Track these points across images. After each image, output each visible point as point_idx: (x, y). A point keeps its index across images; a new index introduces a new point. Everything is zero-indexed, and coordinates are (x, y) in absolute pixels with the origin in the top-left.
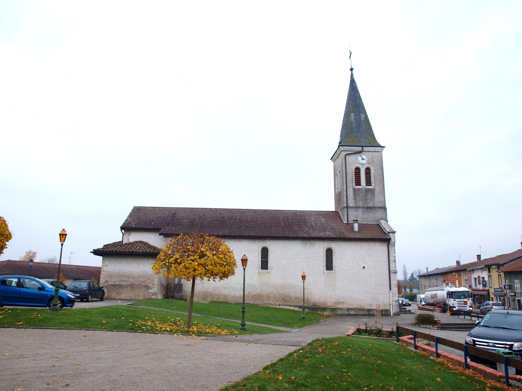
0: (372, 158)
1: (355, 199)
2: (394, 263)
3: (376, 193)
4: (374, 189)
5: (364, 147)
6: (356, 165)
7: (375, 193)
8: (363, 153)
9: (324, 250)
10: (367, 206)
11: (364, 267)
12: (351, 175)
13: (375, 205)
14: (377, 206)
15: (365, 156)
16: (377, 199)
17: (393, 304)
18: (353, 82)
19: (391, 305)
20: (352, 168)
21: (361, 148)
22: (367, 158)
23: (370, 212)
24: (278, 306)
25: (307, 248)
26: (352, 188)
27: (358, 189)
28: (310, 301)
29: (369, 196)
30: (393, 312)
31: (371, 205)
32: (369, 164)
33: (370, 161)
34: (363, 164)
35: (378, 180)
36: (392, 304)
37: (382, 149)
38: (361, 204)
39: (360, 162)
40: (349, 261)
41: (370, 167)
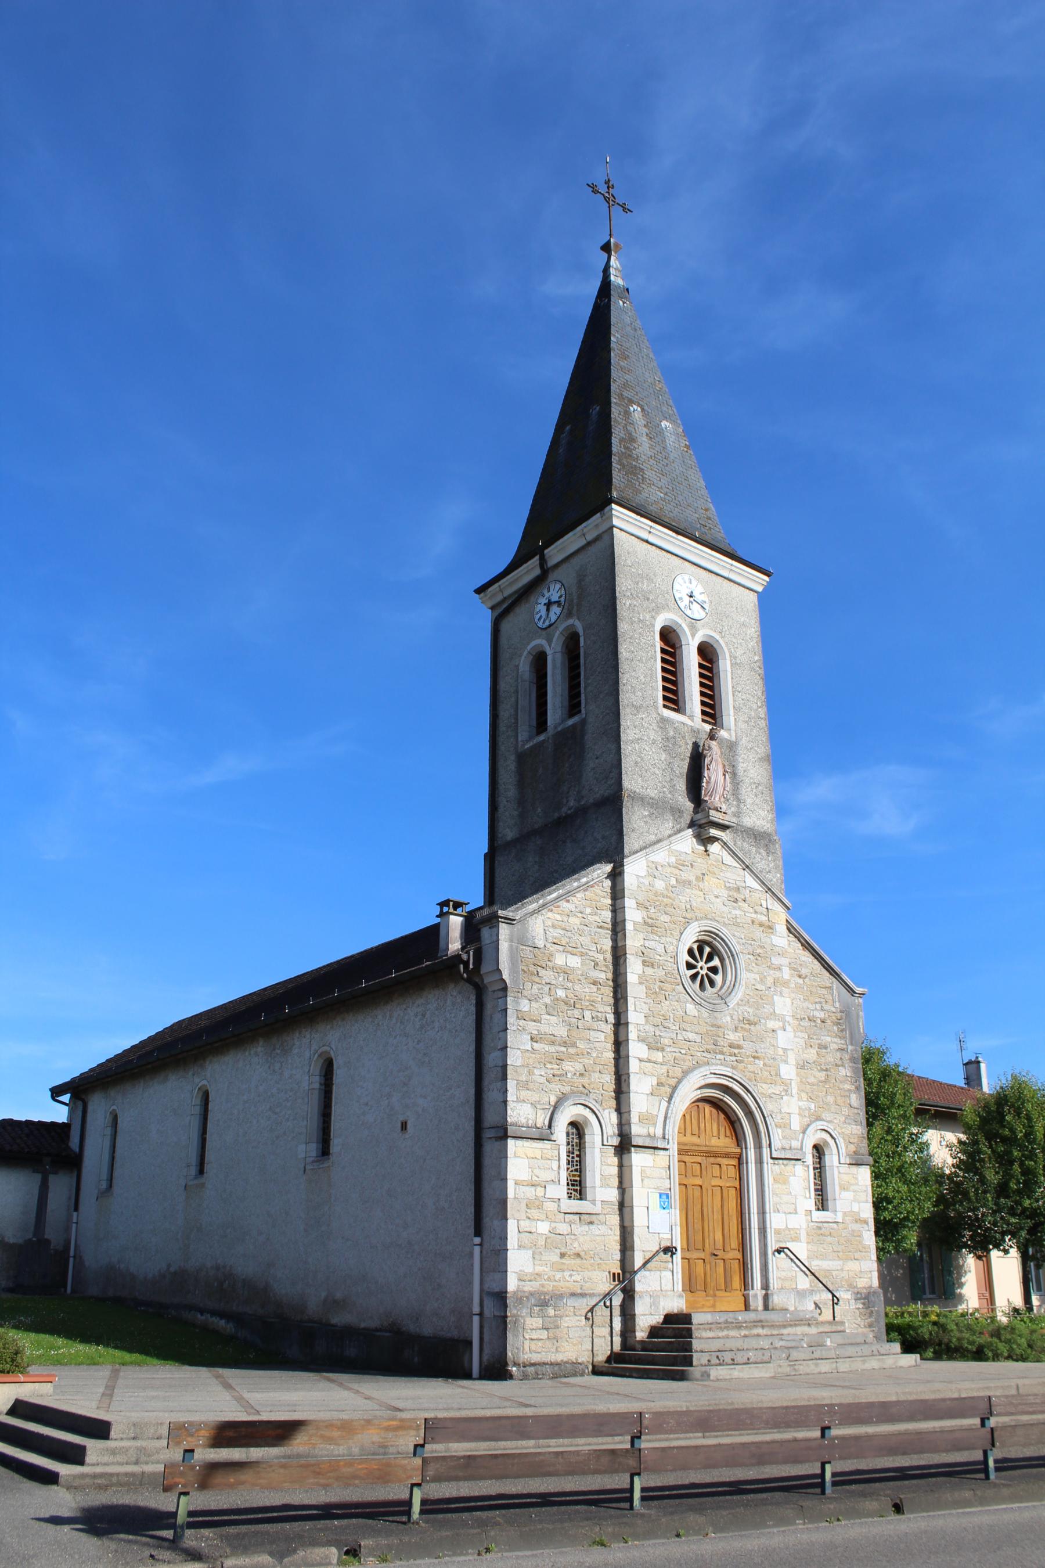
0: (581, 579)
1: (521, 802)
2: (499, 1084)
3: (589, 737)
4: (583, 722)
5: (546, 551)
6: (528, 644)
7: (586, 737)
8: (552, 576)
9: (310, 1066)
10: (556, 815)
11: (404, 1126)
12: (513, 699)
13: (583, 797)
14: (591, 801)
15: (558, 586)
16: (592, 765)
17: (487, 1313)
18: (606, 287)
19: (476, 1320)
20: (517, 666)
21: (536, 560)
22: (563, 592)
23: (564, 842)
24: (199, 1316)
25: (274, 1071)
26: (513, 757)
27: (531, 747)
28: (271, 1295)
29: (567, 765)
30: (485, 1358)
31: (572, 803)
32: (569, 615)
33: (572, 601)
34: (551, 625)
35: (599, 670)
36: (481, 1314)
37: (604, 518)
38: (538, 817)
39: (540, 624)
40: (367, 1104)
41: (573, 625)
